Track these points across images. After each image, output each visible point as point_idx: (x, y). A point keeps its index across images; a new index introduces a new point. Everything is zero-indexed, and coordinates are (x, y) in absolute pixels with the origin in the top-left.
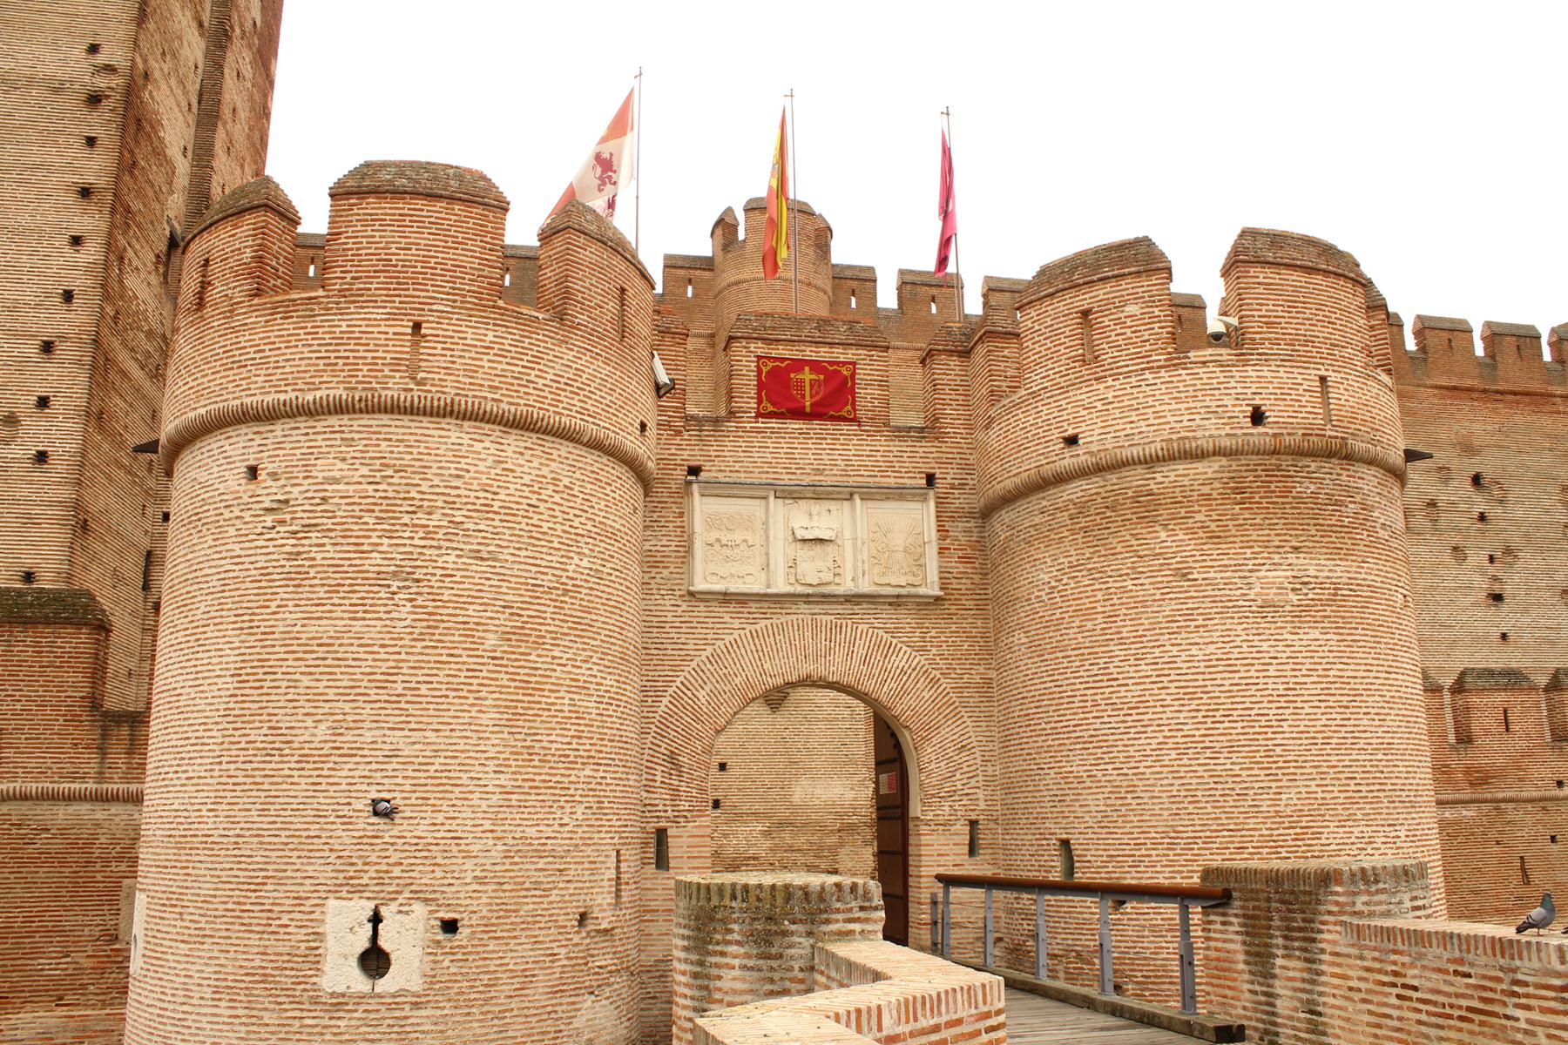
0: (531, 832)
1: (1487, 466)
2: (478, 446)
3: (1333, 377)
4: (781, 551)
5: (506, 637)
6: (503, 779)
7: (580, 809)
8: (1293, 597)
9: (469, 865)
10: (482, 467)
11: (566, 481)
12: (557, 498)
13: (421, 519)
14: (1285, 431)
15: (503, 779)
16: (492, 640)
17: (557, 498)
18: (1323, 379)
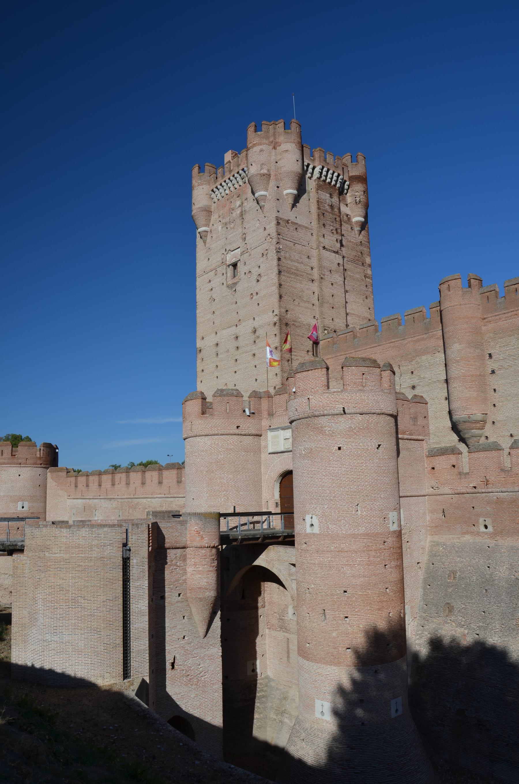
0: (212, 503)
2: (201, 440)
3: (311, 397)
4: (282, 441)
5: (207, 472)
6: (207, 495)
7: (222, 499)
8: (303, 452)
9: (203, 508)
10: (202, 444)
11: (217, 443)
12: (215, 446)
13: (195, 454)
14: (300, 414)
15: (207, 495)
16: (205, 472)
17: (215, 446)
18: (309, 399)
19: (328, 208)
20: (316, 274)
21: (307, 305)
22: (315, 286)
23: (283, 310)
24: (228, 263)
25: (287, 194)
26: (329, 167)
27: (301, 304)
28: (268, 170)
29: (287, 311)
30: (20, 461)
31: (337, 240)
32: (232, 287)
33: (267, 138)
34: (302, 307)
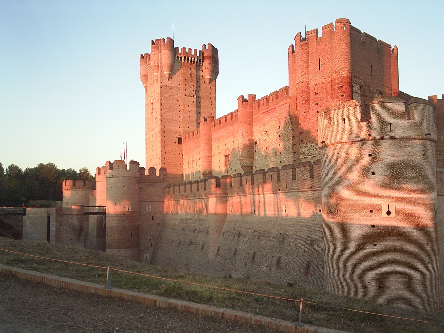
1: (266, 128)
19: (189, 76)
20: (181, 108)
21: (175, 122)
22: (180, 114)
23: (163, 126)
24: (152, 102)
25: (166, 74)
26: (188, 56)
27: (173, 122)
28: (158, 63)
29: (165, 126)
30: (76, 188)
31: (193, 90)
32: (152, 113)
33: (157, 48)
34: (173, 123)
